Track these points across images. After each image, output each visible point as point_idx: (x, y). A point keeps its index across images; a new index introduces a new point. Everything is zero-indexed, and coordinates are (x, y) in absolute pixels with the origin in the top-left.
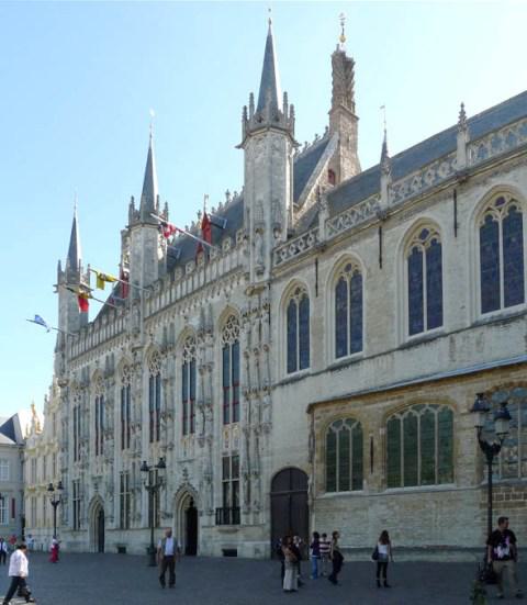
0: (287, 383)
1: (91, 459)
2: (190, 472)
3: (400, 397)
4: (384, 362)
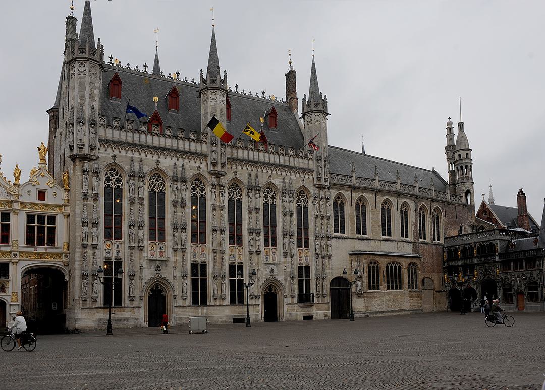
0: (339, 238)
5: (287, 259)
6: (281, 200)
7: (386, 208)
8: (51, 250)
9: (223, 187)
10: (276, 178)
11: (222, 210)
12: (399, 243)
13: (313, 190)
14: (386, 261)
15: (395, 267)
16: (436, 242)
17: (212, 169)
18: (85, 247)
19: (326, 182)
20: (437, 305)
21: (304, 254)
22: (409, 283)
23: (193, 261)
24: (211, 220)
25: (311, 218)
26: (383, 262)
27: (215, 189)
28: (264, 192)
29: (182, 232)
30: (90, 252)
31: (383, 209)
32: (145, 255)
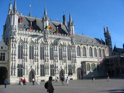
8: (4, 62)
13: (71, 45)
26: (90, 63)
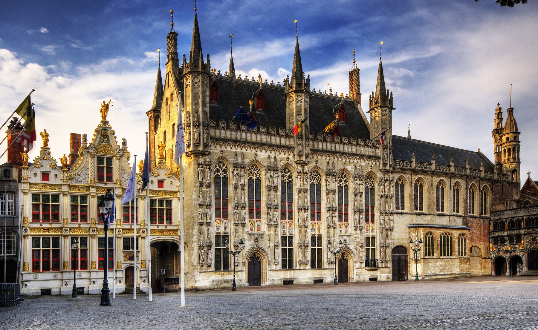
0: (400, 214)
1: (247, 220)
2: (348, 241)
3: (444, 230)
4: (433, 217)
5: (357, 231)
6: (353, 183)
7: (440, 187)
9: (307, 173)
10: (349, 165)
11: (306, 192)
12: (451, 217)
14: (440, 232)
15: (448, 237)
16: (483, 215)
17: (298, 159)
18: (201, 224)
19: (390, 167)
20: (483, 270)
21: (370, 228)
22: (459, 250)
23: (283, 234)
24: (297, 201)
25: (377, 197)
27: (301, 176)
28: (339, 177)
29: (274, 211)
30: (205, 228)
31: (438, 188)
32: (246, 230)
